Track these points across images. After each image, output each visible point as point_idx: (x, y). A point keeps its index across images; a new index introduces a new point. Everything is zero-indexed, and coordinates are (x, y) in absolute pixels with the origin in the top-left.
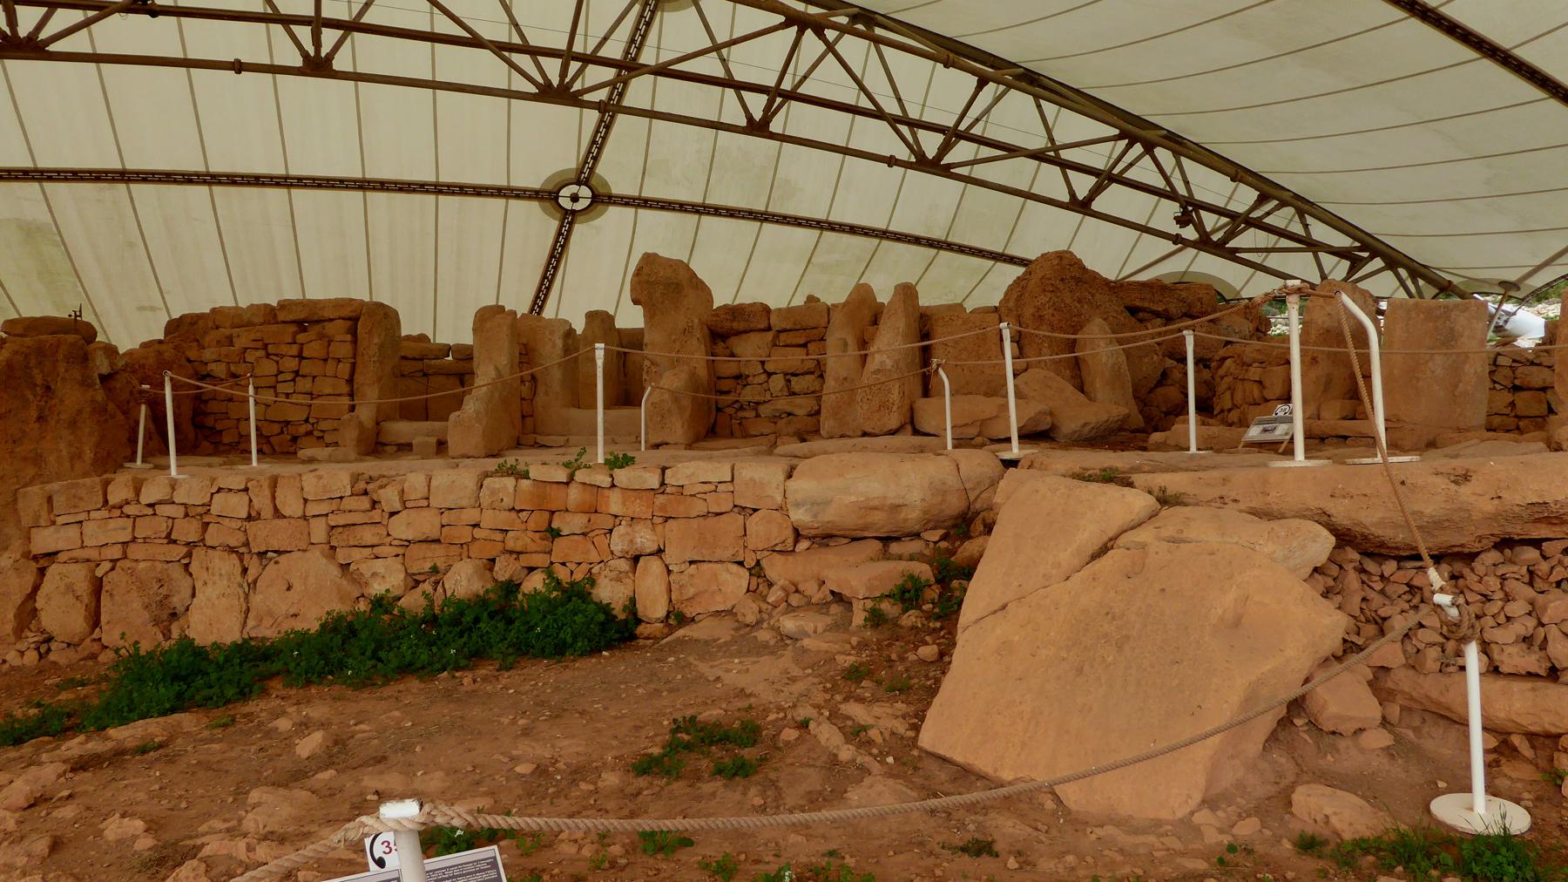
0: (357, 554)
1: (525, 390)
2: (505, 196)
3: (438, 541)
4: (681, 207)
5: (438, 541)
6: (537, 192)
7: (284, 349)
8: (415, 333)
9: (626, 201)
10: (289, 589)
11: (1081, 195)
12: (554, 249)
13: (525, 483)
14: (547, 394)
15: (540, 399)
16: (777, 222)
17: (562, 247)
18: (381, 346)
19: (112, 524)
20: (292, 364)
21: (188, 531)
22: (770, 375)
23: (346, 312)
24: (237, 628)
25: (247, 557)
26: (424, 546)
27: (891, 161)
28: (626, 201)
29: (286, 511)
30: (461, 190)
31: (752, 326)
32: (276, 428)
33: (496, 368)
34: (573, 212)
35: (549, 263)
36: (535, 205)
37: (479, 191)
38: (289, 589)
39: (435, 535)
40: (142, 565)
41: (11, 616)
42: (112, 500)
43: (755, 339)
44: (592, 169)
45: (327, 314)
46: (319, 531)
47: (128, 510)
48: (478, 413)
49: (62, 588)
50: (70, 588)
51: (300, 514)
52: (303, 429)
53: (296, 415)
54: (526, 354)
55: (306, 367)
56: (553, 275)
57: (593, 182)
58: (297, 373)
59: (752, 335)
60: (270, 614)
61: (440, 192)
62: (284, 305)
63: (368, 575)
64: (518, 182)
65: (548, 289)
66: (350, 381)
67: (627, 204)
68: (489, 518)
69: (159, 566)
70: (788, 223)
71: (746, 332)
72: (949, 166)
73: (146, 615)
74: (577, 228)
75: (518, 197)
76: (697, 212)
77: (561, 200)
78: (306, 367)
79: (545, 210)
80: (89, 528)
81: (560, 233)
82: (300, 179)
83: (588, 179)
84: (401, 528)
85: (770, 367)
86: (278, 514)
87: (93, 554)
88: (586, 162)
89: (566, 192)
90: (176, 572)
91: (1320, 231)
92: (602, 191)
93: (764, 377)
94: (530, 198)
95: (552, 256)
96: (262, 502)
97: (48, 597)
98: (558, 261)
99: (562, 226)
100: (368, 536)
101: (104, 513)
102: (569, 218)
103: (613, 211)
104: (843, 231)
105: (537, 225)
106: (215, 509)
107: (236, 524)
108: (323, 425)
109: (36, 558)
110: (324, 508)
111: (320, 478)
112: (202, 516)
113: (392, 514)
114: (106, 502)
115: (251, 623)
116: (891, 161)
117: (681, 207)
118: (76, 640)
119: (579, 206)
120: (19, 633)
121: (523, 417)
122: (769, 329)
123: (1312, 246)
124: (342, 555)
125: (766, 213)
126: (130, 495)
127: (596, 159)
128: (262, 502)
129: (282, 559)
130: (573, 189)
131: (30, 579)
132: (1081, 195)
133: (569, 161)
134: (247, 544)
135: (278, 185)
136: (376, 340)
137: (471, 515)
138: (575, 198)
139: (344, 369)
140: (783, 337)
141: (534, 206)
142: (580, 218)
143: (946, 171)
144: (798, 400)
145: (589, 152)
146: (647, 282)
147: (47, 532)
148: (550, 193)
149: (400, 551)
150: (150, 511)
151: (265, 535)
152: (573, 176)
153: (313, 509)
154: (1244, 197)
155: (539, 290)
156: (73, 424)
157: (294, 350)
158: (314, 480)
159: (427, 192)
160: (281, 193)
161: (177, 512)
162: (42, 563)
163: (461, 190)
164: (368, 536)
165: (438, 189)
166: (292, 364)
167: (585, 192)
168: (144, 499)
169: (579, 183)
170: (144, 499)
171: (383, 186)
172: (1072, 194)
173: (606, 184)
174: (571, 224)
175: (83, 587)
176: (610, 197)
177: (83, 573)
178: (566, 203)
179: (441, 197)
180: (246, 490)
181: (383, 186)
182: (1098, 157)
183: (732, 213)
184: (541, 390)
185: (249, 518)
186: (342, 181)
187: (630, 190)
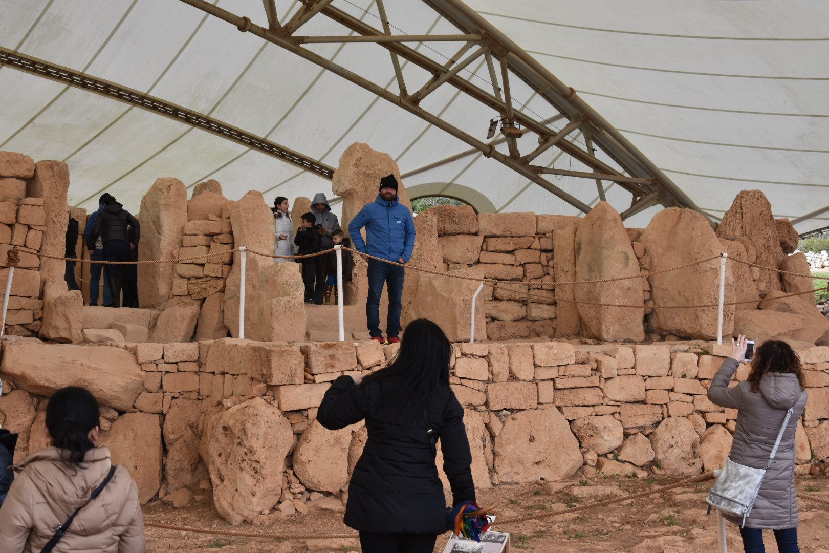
0: (582, 412)
3: (644, 402)
5: (644, 402)
10: (532, 440)
11: (411, 92)
13: (706, 358)
16: (22, 67)
23: (24, 171)
26: (634, 406)
27: (244, 25)
29: (521, 375)
31: (465, 229)
38: (532, 440)
39: (641, 396)
46: (547, 391)
49: (332, 441)
51: (531, 378)
59: (461, 238)
63: (601, 427)
68: (682, 386)
70: (35, 71)
71: (452, 234)
72: (302, 40)
84: (615, 391)
86: (513, 377)
91: (601, 155)
96: (501, 367)
100: (590, 397)
104: (96, 89)
107: (476, 385)
109: (287, 414)
110: (553, 373)
111: (551, 348)
113: (607, 379)
116: (244, 25)
122: (476, 234)
123: (601, 171)
124: (569, 413)
125: (14, 54)
128: (501, 367)
129: (518, 415)
132: (411, 92)
134: (486, 404)
137: (668, 382)
140: (492, 242)
143: (295, 45)
144: (503, 305)
146: (364, 174)
149: (617, 409)
153: (543, 374)
154: (540, 110)
158: (545, 350)
162: (295, 418)
164: (590, 397)
182: (440, 54)
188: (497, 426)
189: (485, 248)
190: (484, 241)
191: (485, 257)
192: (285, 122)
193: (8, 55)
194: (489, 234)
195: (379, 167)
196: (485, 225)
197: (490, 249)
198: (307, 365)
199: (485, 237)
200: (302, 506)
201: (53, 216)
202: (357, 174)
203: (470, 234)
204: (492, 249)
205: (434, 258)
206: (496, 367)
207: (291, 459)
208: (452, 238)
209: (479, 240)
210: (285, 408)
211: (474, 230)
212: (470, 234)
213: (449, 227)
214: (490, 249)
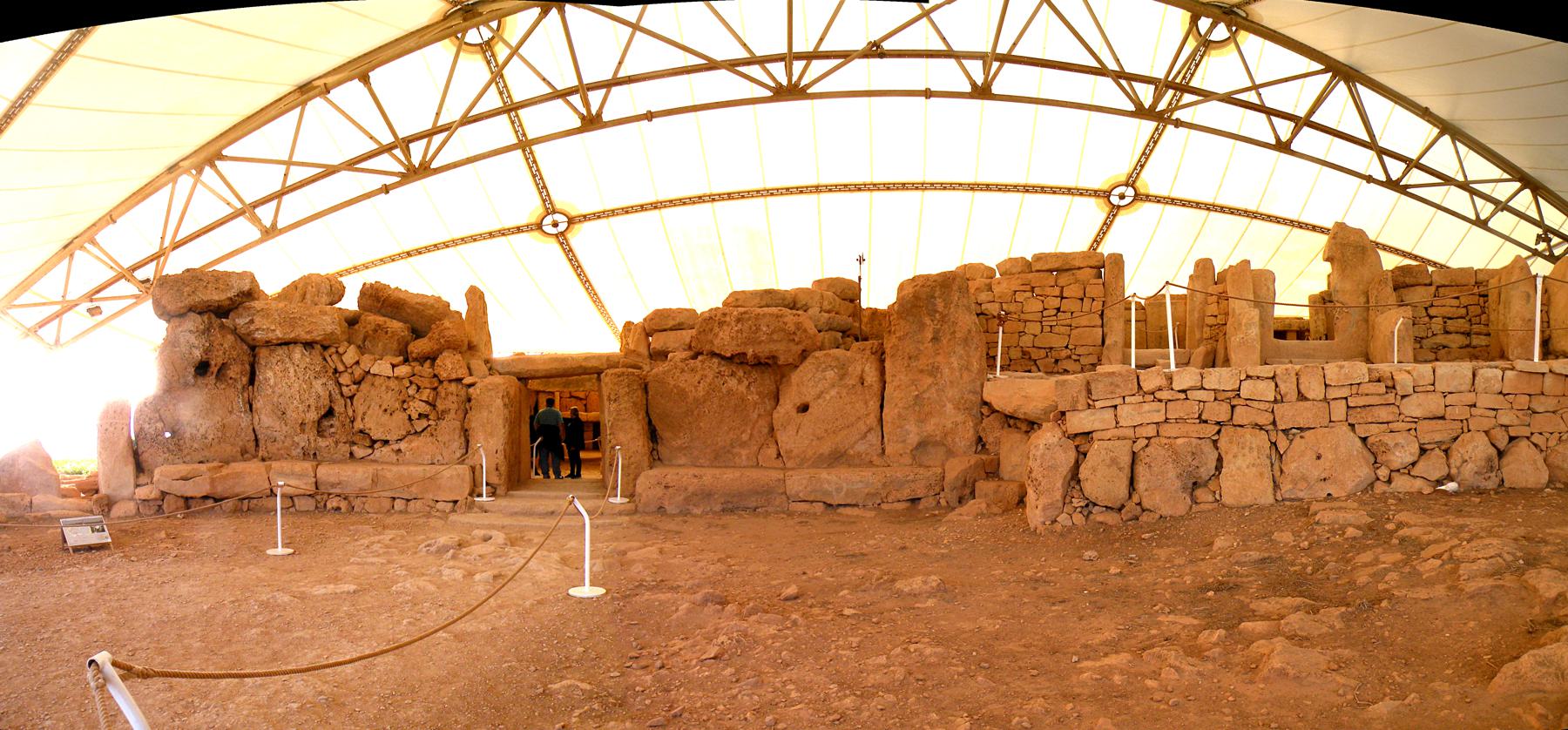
7: (1049, 291)
19: (1146, 407)
20: (1056, 302)
21: (1220, 412)
24: (1270, 490)
25: (1273, 434)
32: (1042, 353)
37: (1054, 191)
40: (1179, 441)
41: (1059, 485)
42: (1146, 386)
45: (1077, 264)
47: (1159, 395)
50: (1114, 461)
52: (1065, 353)
53: (1057, 342)
55: (1065, 305)
58: (1058, 310)
60: (1304, 478)
62: (1039, 258)
66: (1102, 316)
69: (1195, 441)
73: (1178, 484)
78: (1065, 305)
80: (1123, 411)
87: (1130, 433)
90: (1207, 447)
97: (1094, 470)
101: (1139, 398)
106: (1244, 393)
107: (1262, 406)
108: (1080, 351)
112: (1233, 399)
114: (1140, 387)
115: (1286, 487)
118: (1118, 505)
120: (1066, 498)
126: (1164, 382)
131: (1072, 455)
139: (1098, 305)
147: (1082, 415)
150: (1183, 396)
151: (1289, 415)
156: (966, 341)
157: (1057, 291)
161: (1209, 396)
166: (1056, 302)
168: (1176, 386)
170: (1176, 386)
175: (1126, 460)
177: (1128, 448)
180: (1273, 378)
185: (1276, 401)
188: (1283, 444)
198: (1089, 392)
200: (1078, 519)
206: (1282, 387)
207: (1074, 476)
210: (1072, 431)
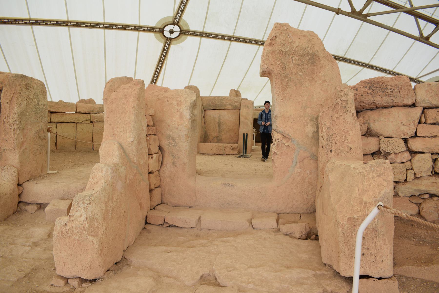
1: (153, 164)
2: (137, 30)
4: (223, 37)
6: (153, 28)
8: (86, 98)
9: (196, 34)
12: (161, 58)
14: (174, 164)
15: (168, 169)
17: (165, 56)
18: (22, 115)
22: (413, 153)
28: (196, 34)
30: (116, 27)
31: (398, 101)
33: (121, 147)
34: (171, 39)
35: (158, 65)
36: (152, 35)
37: (125, 28)
43: (399, 114)
44: (180, 16)
48: (91, 220)
54: (154, 126)
56: (160, 70)
57: (181, 23)
59: (394, 111)
61: (106, 28)
64: (145, 23)
65: (157, 77)
67: (196, 35)
71: (385, 107)
74: (172, 47)
75: (144, 30)
76: (230, 40)
77: (165, 33)
79: (157, 38)
81: (164, 50)
82: (36, 21)
83: (178, 22)
85: (415, 145)
88: (178, 13)
89: (168, 28)
92: (184, 28)
93: (407, 155)
94: (150, 31)
95: (160, 61)
98: (162, 64)
99: (165, 46)
102: (168, 41)
103: (190, 38)
105: (153, 44)
117: (223, 37)
119: (173, 36)
121: (151, 191)
122: (414, 105)
127: (182, 11)
130: (170, 27)
133: (169, 12)
135: (26, 23)
136: (16, 109)
138: (172, 32)
140: (432, 115)
141: (152, 35)
142: (173, 42)
145: (180, 8)
146: (281, 52)
148: (160, 29)
152: (171, 20)
155: (154, 78)
159: (100, 27)
160: (28, 27)
163: (116, 27)
165: (105, 26)
167: (176, 29)
169: (174, 24)
171: (78, 24)
172: (421, 34)
173: (187, 25)
174: (169, 45)
176: (189, 32)
178: (167, 34)
179: (107, 30)
181: (78, 24)
183: (246, 41)
184: (168, 160)
186: (57, 22)
187: (200, 29)
189: (423, 120)
190: (423, 113)
191: (423, 130)
192: (375, 56)
193: (260, 42)
194: (428, 105)
195: (297, 43)
196: (424, 97)
197: (429, 122)
199: (424, 108)
201: (4, 118)
202: (272, 53)
203: (405, 106)
204: (432, 122)
205: (349, 138)
208: (385, 111)
209: (417, 111)
211: (410, 102)
212: (405, 106)
213: (379, 100)
214: (429, 122)
